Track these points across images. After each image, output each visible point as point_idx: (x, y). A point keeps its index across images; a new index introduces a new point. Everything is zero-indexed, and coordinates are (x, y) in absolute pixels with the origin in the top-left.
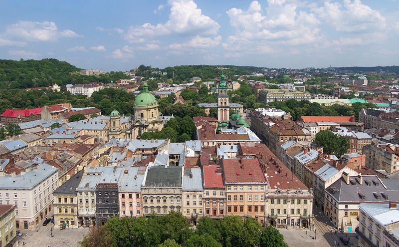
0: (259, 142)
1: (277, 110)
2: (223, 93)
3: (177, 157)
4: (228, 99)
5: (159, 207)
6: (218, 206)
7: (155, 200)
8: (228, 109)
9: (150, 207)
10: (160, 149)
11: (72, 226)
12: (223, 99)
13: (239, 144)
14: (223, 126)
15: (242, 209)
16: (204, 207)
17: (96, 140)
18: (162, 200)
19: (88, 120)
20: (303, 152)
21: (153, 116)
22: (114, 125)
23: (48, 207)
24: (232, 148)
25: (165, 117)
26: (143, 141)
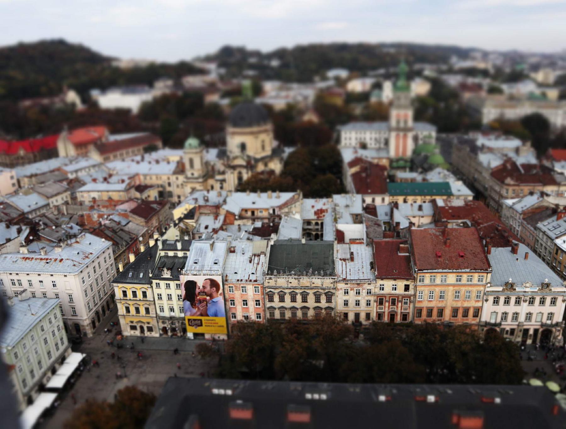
0: (471, 198)
3: (317, 224)
5: (293, 308)
7: (288, 298)
9: (279, 308)
10: (286, 210)
11: (149, 333)
12: (402, 112)
13: (434, 202)
14: (399, 168)
15: (441, 312)
16: (374, 310)
17: (161, 194)
18: (299, 298)
20: (555, 218)
23: (105, 303)
24: (420, 208)
25: (288, 150)
26: (253, 196)
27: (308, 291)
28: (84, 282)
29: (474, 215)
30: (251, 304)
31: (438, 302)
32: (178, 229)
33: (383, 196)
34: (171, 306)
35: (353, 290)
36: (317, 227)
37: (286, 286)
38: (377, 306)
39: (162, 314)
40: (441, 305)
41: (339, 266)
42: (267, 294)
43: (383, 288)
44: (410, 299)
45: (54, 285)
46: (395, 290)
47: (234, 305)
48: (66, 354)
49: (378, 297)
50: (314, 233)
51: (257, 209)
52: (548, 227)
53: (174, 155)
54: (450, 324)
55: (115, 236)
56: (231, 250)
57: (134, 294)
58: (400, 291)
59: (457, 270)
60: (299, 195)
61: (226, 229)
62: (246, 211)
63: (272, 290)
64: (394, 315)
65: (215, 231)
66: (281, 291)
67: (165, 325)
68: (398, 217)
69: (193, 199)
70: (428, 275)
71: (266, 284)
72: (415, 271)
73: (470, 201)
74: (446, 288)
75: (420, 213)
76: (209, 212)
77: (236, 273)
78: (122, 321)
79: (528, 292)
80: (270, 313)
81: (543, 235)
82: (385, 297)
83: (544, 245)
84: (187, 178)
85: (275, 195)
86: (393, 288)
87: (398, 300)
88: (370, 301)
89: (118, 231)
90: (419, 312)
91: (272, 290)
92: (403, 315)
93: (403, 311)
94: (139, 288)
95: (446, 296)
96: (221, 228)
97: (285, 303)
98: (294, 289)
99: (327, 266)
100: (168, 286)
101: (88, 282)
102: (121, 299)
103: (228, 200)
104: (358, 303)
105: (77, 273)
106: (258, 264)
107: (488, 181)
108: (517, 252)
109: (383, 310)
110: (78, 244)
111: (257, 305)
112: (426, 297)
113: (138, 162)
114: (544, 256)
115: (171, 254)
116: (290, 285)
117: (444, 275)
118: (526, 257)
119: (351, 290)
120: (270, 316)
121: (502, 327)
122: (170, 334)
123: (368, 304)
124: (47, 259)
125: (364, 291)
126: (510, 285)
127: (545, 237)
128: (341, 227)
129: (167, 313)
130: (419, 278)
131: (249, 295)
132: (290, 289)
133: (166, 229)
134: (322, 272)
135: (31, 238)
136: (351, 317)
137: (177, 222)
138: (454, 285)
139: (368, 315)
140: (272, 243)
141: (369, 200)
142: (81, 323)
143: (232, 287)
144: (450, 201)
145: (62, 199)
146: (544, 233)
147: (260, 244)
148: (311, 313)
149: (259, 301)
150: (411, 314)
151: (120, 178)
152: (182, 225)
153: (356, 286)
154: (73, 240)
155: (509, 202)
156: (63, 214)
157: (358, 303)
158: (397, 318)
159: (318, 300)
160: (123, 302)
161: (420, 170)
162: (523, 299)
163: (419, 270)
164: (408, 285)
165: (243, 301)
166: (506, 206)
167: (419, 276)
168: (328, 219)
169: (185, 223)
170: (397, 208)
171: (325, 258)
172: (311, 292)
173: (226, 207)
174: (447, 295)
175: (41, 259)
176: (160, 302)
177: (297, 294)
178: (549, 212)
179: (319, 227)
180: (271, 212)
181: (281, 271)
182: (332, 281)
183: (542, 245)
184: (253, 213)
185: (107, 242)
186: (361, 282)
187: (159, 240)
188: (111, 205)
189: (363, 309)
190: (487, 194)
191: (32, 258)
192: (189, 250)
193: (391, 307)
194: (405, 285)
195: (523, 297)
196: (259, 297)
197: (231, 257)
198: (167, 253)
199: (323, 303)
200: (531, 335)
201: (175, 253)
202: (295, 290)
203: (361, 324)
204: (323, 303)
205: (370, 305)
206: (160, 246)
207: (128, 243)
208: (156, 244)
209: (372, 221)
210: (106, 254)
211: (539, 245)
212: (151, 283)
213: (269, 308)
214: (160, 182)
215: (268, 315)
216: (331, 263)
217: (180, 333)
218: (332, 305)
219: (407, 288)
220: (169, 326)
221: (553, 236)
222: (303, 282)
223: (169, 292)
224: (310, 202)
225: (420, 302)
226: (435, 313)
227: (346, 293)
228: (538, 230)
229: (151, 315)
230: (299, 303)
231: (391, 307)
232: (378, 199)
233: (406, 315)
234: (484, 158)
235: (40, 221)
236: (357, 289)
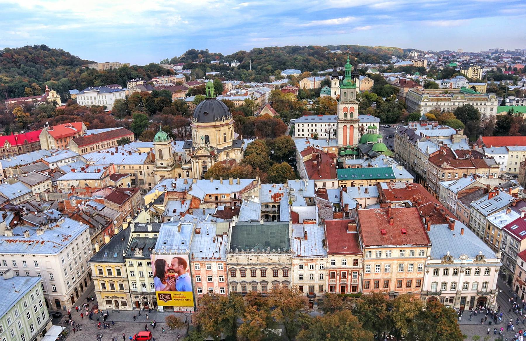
1: (439, 127)
2: (349, 97)
3: (274, 207)
4: (356, 107)
6: (349, 281)
7: (248, 273)
8: (356, 126)
9: (241, 283)
10: (246, 195)
11: (123, 307)
12: (349, 106)
13: (378, 185)
16: (326, 283)
17: (134, 182)
18: (259, 273)
19: (117, 149)
21: (225, 141)
22: (161, 157)
23: (83, 281)
27: (266, 267)
28: (63, 261)
29: (415, 196)
30: (216, 279)
31: (384, 274)
32: (149, 213)
33: (333, 181)
34: (143, 282)
35: (308, 265)
36: (274, 209)
37: (247, 262)
38: (329, 279)
39: (133, 290)
40: (386, 277)
41: (294, 244)
42: (229, 270)
43: (334, 263)
44: (359, 272)
45: (36, 265)
46: (345, 264)
47: (200, 280)
48: (47, 327)
49: (329, 271)
50: (271, 215)
51: (220, 194)
53: (145, 147)
54: (395, 294)
55: (91, 219)
56: (197, 232)
57: (110, 272)
58: (350, 265)
59: (400, 245)
60: (258, 182)
61: (192, 212)
62: (210, 196)
63: (234, 266)
64: (345, 287)
65: (182, 215)
66: (243, 268)
67: (138, 300)
68: (347, 198)
69: (162, 186)
70: (374, 251)
71: (229, 261)
72: (363, 247)
73: (411, 184)
74: (391, 262)
75: (367, 195)
76: (177, 197)
77: (201, 252)
78: (98, 296)
80: (233, 287)
82: (336, 271)
84: (156, 167)
85: (235, 181)
86: (343, 263)
87: (348, 274)
88: (322, 275)
89: (94, 215)
90: (367, 284)
91: (234, 266)
92: (353, 287)
93: (352, 283)
94: (114, 267)
95: (391, 269)
96: (188, 212)
97: (246, 278)
98: (254, 265)
99: (283, 244)
100: (140, 264)
101: (67, 261)
102: (97, 277)
103: (194, 186)
104: (312, 277)
105: (57, 254)
106: (221, 243)
107: (425, 165)
109: (335, 283)
110: (58, 227)
111: (220, 280)
112: (373, 270)
113: (112, 154)
115: (142, 235)
116: (250, 262)
117: (388, 250)
119: (306, 265)
120: (233, 290)
122: (142, 307)
123: (321, 278)
124: (30, 241)
125: (317, 266)
128: (295, 209)
129: (139, 289)
130: (366, 253)
131: (213, 271)
132: (250, 265)
133: (138, 213)
134: (279, 250)
135: (15, 222)
136: (306, 290)
137: (148, 207)
138: (397, 259)
139: (321, 288)
140: (233, 224)
141: (320, 184)
142: (61, 299)
143: (198, 264)
144: (393, 184)
145: (44, 187)
147: (222, 224)
148: (270, 287)
149: (223, 276)
150: (360, 286)
151: (97, 168)
152: (152, 209)
153: (310, 261)
154: (54, 224)
155: (446, 184)
156: (45, 201)
157: (312, 277)
158: (347, 290)
159: (276, 275)
160: (99, 279)
161: (366, 157)
163: (366, 246)
164: (357, 260)
165: (208, 277)
166: (443, 187)
167: (366, 251)
168: (283, 203)
169: (155, 208)
170: (346, 191)
171: (281, 237)
172: (269, 268)
173: (191, 193)
174: (392, 268)
175: (25, 241)
176: (133, 279)
177: (256, 270)
179: (276, 209)
180: (233, 196)
181: (242, 250)
182: (288, 257)
184: (216, 198)
185: (84, 225)
186: (314, 258)
187: (132, 223)
188: (88, 192)
189: (316, 282)
190: (425, 177)
191: (17, 241)
192: (159, 232)
193: (341, 279)
194: (354, 260)
196: (223, 273)
197: (197, 238)
198: (139, 235)
199: (281, 277)
201: (146, 235)
202: (254, 267)
203: (315, 296)
204: (281, 277)
205: (322, 278)
206: (133, 229)
207: (104, 226)
208: (129, 227)
209: (323, 203)
210: (84, 237)
212: (124, 262)
213: (231, 283)
214: (132, 171)
215: (231, 289)
216: (287, 241)
217: (152, 306)
218: (289, 279)
219: (356, 262)
220: (141, 301)
222: (262, 259)
223: (141, 269)
224: (268, 187)
225: (367, 274)
226: (381, 284)
227: (301, 268)
229: (124, 291)
230: (259, 278)
231: (341, 279)
232: (329, 183)
233: (356, 287)
234: (421, 145)
235: (24, 206)
236: (310, 264)
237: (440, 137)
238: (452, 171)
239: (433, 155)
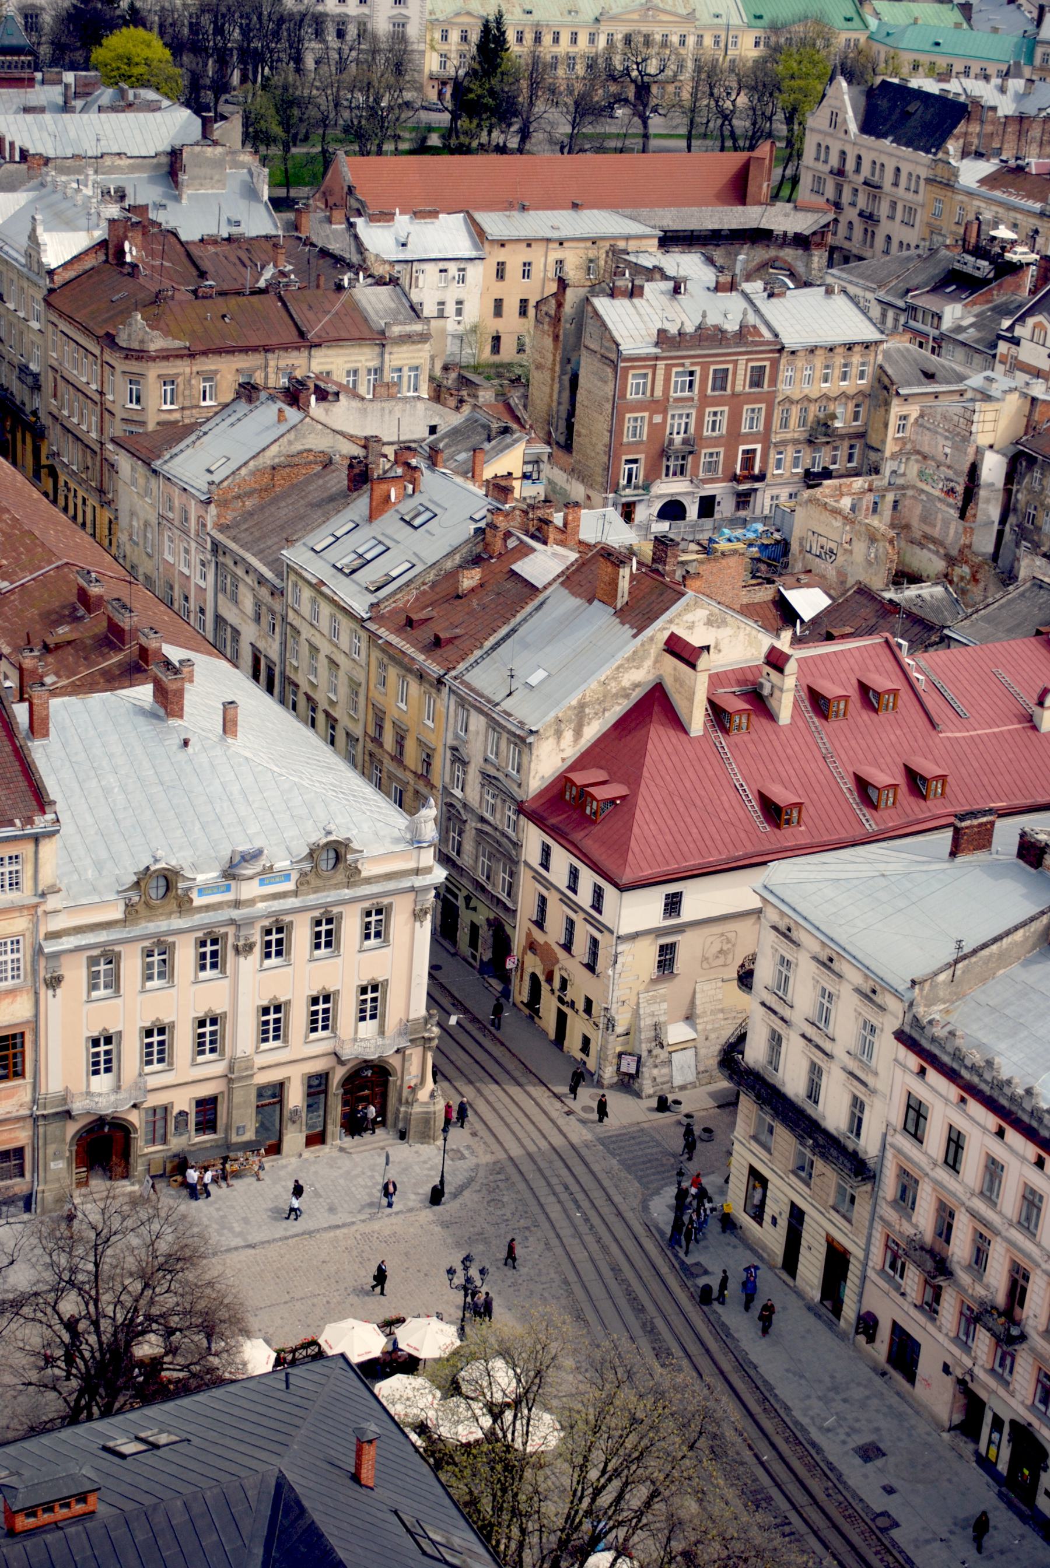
1: (106, 95)
20: (361, 504)
52: (331, 555)
79: (252, 902)
81: (314, 601)
83: (325, 648)
108: (182, 709)
114: (332, 703)
118: (229, 725)
121: (153, 1100)
126: (162, 882)
127: (325, 609)
146: (317, 587)
162: (231, 941)
178: (340, 479)
183: (314, 649)
195: (231, 930)
200: (296, 1112)
211: (305, 649)
221: (360, 606)
228: (293, 577)
237: (108, 161)
238: (182, 368)
239: (70, 274)
